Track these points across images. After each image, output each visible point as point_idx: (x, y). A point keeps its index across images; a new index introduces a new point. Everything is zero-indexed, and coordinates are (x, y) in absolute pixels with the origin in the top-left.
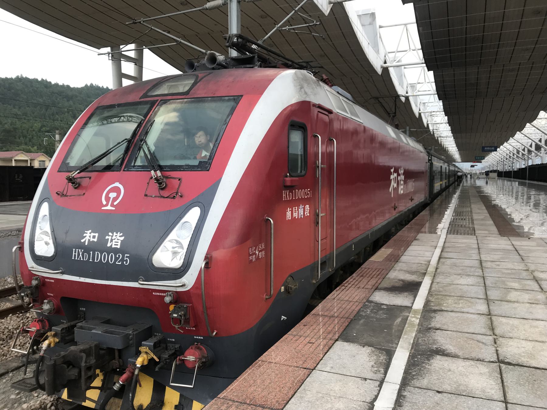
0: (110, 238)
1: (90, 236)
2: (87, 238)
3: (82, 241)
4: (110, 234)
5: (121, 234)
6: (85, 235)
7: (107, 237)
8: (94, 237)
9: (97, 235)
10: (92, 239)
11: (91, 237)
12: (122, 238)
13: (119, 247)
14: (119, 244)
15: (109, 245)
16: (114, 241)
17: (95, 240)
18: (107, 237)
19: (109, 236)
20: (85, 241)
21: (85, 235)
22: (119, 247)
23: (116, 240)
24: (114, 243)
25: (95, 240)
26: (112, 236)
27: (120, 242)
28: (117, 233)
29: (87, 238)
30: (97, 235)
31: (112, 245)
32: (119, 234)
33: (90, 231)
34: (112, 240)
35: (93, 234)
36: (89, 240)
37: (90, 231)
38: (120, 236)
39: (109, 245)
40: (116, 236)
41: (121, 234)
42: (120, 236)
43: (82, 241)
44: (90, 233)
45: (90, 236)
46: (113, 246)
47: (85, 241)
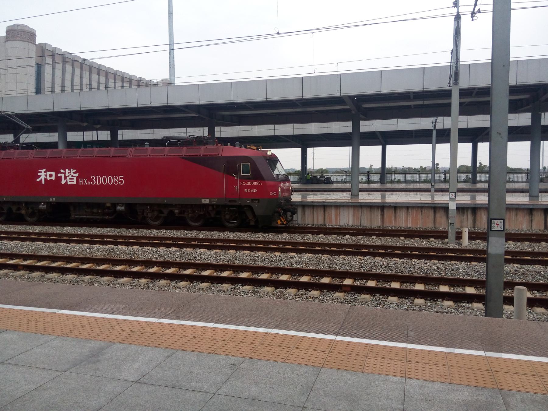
0: (63, 175)
1: (46, 175)
2: (43, 177)
4: (62, 171)
5: (75, 171)
6: (39, 174)
9: (53, 173)
10: (49, 178)
11: (48, 176)
12: (77, 175)
13: (75, 183)
14: (75, 180)
15: (63, 182)
16: (68, 178)
17: (53, 178)
19: (62, 173)
20: (42, 180)
22: (75, 183)
23: (70, 177)
24: (68, 180)
25: (53, 178)
26: (65, 174)
27: (75, 178)
28: (69, 170)
29: (43, 177)
30: (53, 173)
32: (72, 171)
33: (45, 170)
34: (65, 178)
35: (48, 173)
36: (46, 180)
37: (45, 170)
38: (74, 173)
39: (63, 182)
40: (69, 173)
41: (75, 171)
42: (74, 173)
43: (38, 180)
44: (45, 172)
45: (46, 175)
46: (69, 183)
47: (42, 180)
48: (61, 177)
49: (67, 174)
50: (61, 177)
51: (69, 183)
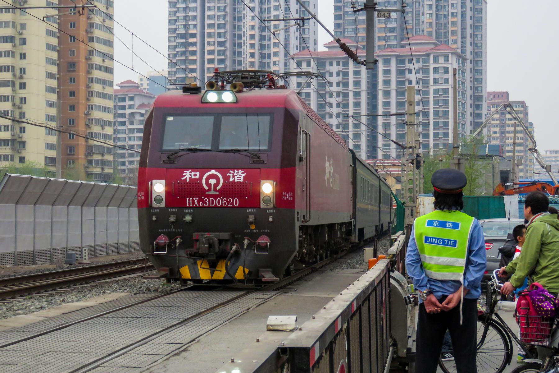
0: (231, 175)
3: (183, 179)
4: (231, 171)
7: (228, 174)
8: (195, 175)
10: (193, 177)
13: (242, 181)
15: (231, 180)
16: (236, 177)
17: (197, 177)
18: (228, 174)
21: (184, 174)
22: (242, 181)
23: (238, 176)
26: (233, 174)
31: (235, 180)
34: (234, 176)
39: (231, 180)
46: (236, 181)
48: (230, 176)
49: (235, 174)
50: (230, 176)
51: (236, 181)
